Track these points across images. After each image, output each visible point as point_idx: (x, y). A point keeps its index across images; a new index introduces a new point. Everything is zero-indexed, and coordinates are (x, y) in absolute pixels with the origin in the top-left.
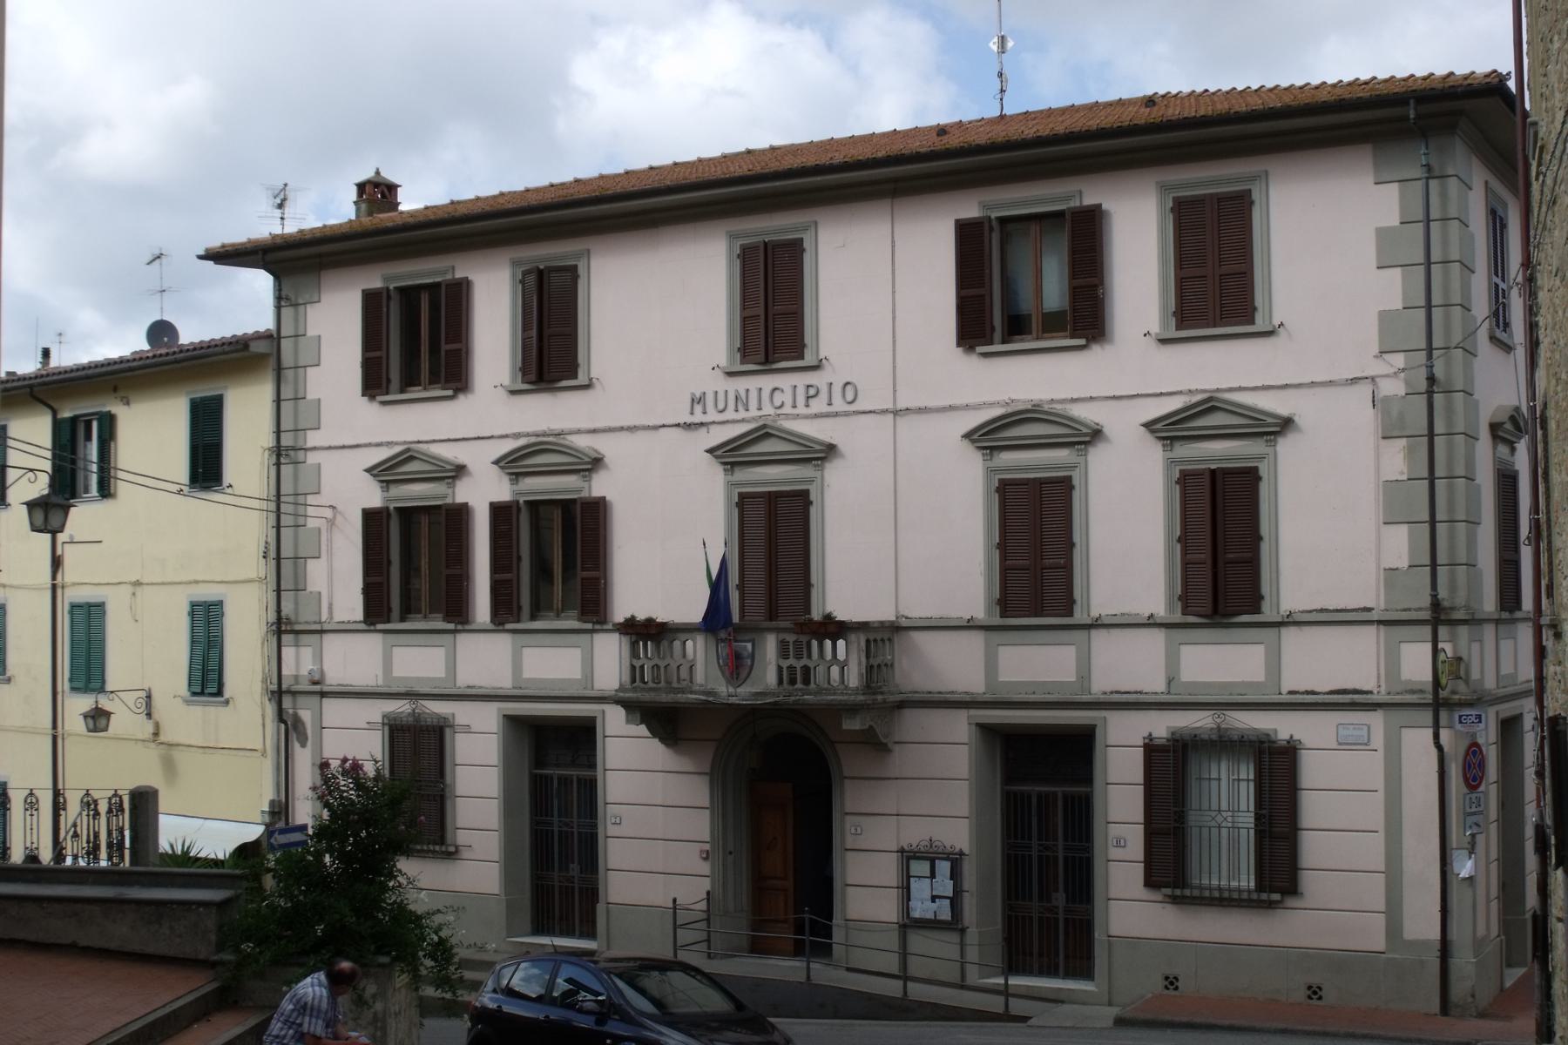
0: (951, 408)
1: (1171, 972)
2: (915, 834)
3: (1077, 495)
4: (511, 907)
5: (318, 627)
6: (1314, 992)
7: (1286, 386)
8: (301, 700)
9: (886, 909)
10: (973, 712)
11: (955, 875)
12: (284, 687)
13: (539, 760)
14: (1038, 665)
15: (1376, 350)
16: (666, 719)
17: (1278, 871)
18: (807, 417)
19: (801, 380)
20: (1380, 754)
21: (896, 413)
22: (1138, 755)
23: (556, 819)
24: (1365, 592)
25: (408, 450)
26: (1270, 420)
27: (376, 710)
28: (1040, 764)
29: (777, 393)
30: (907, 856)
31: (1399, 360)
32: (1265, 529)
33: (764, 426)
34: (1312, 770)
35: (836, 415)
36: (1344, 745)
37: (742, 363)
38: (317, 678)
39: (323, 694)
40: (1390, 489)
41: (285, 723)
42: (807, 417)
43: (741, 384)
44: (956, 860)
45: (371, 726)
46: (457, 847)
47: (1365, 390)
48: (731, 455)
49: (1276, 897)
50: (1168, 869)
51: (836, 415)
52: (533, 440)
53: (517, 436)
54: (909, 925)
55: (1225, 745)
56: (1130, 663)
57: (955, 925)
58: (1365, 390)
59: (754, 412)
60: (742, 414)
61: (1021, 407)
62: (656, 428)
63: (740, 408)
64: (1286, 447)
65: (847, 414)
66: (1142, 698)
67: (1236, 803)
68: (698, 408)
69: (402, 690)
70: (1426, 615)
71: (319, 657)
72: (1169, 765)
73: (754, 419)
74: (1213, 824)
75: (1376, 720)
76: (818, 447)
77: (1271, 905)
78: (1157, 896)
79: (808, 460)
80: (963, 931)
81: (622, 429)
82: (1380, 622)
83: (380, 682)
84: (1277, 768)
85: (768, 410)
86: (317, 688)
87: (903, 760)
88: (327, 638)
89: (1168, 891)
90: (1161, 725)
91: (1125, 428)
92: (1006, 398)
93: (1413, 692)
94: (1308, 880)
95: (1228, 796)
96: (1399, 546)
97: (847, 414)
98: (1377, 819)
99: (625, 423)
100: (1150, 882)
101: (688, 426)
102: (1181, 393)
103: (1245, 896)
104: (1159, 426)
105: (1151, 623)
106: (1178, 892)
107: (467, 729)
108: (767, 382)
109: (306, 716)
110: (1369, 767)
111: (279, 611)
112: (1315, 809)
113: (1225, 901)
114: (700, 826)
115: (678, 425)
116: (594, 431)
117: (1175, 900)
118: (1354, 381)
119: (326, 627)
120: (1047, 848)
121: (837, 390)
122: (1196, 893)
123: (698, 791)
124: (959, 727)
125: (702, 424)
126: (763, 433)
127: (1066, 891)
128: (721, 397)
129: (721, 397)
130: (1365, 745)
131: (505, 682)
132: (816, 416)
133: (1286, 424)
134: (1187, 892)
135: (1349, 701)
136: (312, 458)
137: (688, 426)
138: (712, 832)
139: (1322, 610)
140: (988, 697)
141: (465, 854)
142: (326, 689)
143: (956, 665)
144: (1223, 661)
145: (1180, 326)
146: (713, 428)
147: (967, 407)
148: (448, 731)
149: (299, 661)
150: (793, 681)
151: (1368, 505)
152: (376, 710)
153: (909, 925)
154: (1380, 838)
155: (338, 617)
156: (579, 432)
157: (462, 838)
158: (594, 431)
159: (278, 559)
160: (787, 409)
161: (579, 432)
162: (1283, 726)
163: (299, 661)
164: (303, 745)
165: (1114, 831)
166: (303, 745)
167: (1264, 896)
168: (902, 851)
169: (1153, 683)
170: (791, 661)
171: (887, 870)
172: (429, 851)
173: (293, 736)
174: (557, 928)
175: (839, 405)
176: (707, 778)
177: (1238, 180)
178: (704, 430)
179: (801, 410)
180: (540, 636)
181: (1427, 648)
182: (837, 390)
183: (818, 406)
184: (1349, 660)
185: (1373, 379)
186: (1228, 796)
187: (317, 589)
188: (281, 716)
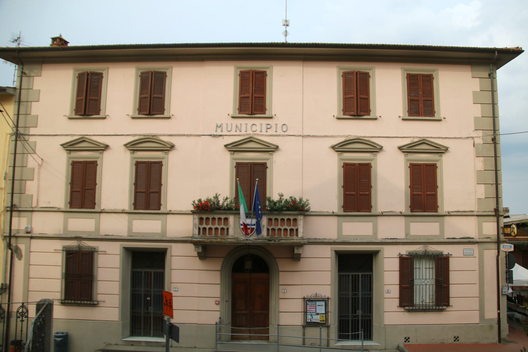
0: (326, 136)
1: (407, 336)
2: (309, 292)
3: (438, 170)
4: (124, 326)
5: (31, 209)
6: (456, 338)
7: (455, 138)
8: (20, 240)
9: (299, 320)
10: (332, 246)
11: (326, 306)
12: (12, 234)
13: (134, 265)
14: (357, 230)
15: (474, 129)
16: (206, 250)
17: (442, 298)
18: (267, 136)
19: (264, 122)
20: (477, 258)
21: (303, 136)
22: (397, 261)
23: (360, 293)
24: (472, 206)
25: (83, 138)
26: (443, 148)
27: (59, 245)
28: (355, 265)
29: (254, 126)
30: (307, 301)
31: (480, 133)
32: (439, 184)
33: (251, 138)
34: (453, 264)
35: (279, 136)
36: (465, 256)
37: (239, 113)
38: (29, 230)
39: (32, 238)
40: (479, 173)
41: (11, 249)
42: (267, 136)
43: (238, 122)
44: (326, 301)
45: (56, 251)
46: (98, 301)
47: (471, 142)
48: (233, 148)
49: (444, 307)
50: (407, 300)
51: (279, 136)
52: (142, 137)
53: (134, 135)
54: (308, 324)
55: (426, 256)
56: (391, 229)
57: (323, 324)
58: (471, 142)
59: (243, 132)
60: (238, 133)
61: (352, 138)
62: (200, 136)
63: (238, 130)
64: (445, 157)
65: (283, 136)
66: (398, 241)
67: (430, 275)
68: (219, 130)
69: (73, 236)
70: (493, 214)
71: (30, 222)
72: (407, 264)
73: (244, 135)
74: (424, 284)
75: (475, 247)
76: (273, 147)
77: (442, 310)
78: (402, 309)
79: (268, 151)
80: (328, 327)
81: (184, 135)
82: (477, 216)
83: (62, 232)
84: (442, 264)
85: (250, 132)
86: (29, 235)
87: (304, 264)
88: (34, 214)
89: (407, 308)
90: (404, 250)
91: (390, 148)
92: (347, 134)
93: (487, 238)
94: (452, 301)
95: (424, 275)
96: (481, 191)
97: (283, 136)
98: (476, 280)
99: (186, 133)
100: (401, 305)
101: (214, 136)
102: (410, 137)
103: (431, 308)
104: (230, 146)
105: (401, 215)
106: (411, 308)
107: (105, 253)
108: (250, 122)
109: (22, 247)
110: (474, 263)
111: (12, 202)
112: (454, 277)
113: (425, 310)
114: (216, 291)
115: (211, 135)
116: (171, 135)
117: (409, 311)
118: (467, 138)
119: (35, 209)
120: (355, 294)
121: (279, 126)
122: (417, 308)
123: (216, 278)
124: (328, 252)
125: (221, 136)
126: (250, 140)
127: (362, 310)
128: (229, 125)
129: (229, 125)
130: (472, 256)
131: (124, 234)
132: (271, 135)
133: (446, 149)
134: (414, 308)
135: (468, 241)
136: (32, 139)
137: (214, 136)
138: (221, 294)
139: (457, 211)
140: (339, 241)
141: (101, 304)
142: (33, 235)
143: (327, 229)
144: (424, 228)
145: (409, 115)
146: (225, 137)
147: (332, 136)
148: (96, 254)
149: (20, 223)
150: (204, 233)
151: (472, 178)
152: (59, 245)
153: (308, 324)
154: (477, 286)
155: (42, 205)
156: (164, 135)
157: (100, 298)
158: (171, 135)
159: (13, 180)
160: (258, 132)
161: (164, 135)
162: (445, 250)
163: (20, 223)
164: (20, 259)
165: (386, 288)
166: (20, 259)
167: (66, 301)
168: (304, 298)
169: (401, 235)
170: (204, 226)
171: (299, 306)
172: (84, 304)
173: (15, 255)
174: (142, 333)
175: (280, 132)
176: (219, 273)
177: (264, 68)
178: (221, 138)
179: (264, 132)
180: (141, 215)
181: (495, 224)
182: (279, 126)
183: (270, 132)
184: (468, 227)
185: (473, 138)
186: (424, 275)
187: (31, 193)
188: (9, 246)
